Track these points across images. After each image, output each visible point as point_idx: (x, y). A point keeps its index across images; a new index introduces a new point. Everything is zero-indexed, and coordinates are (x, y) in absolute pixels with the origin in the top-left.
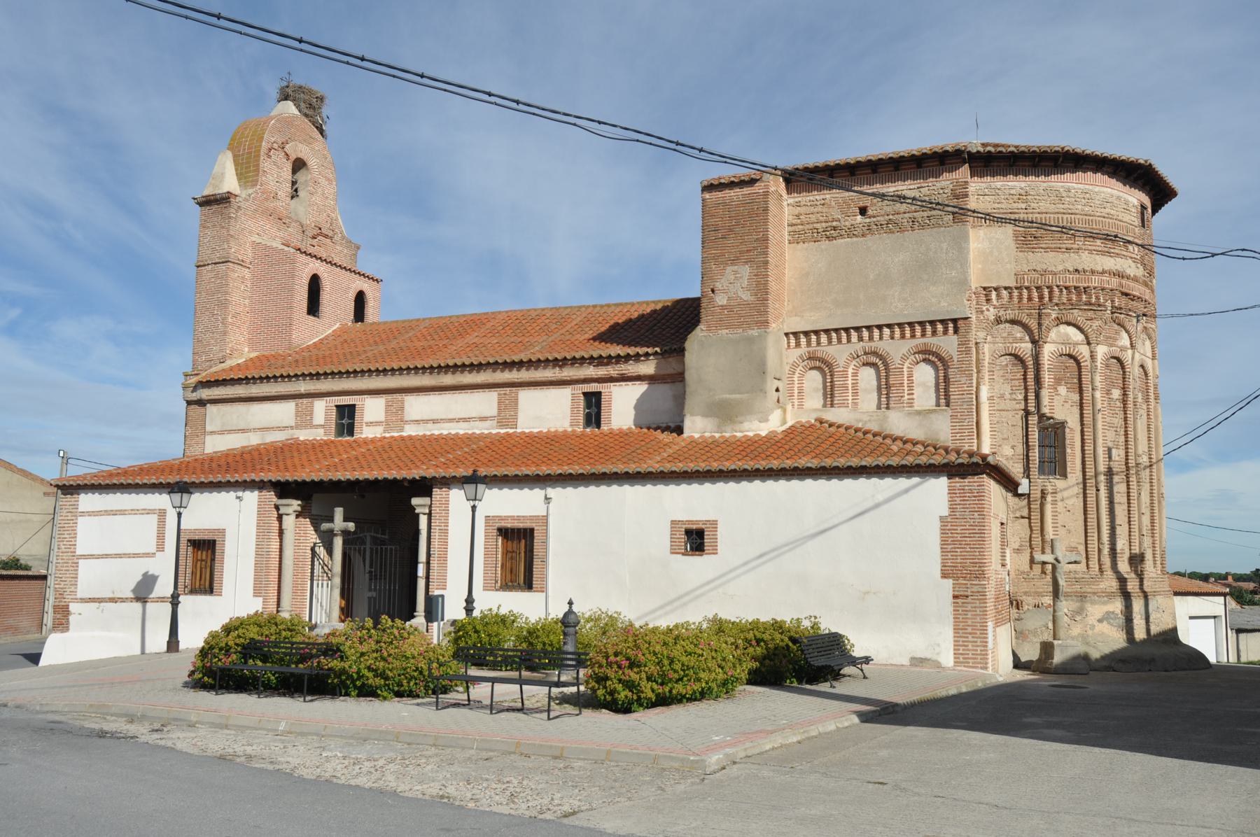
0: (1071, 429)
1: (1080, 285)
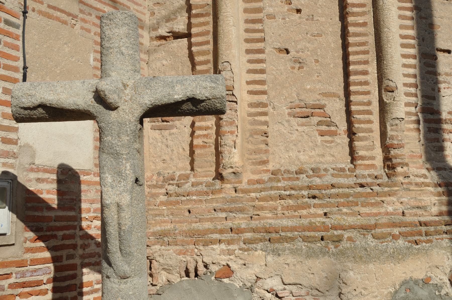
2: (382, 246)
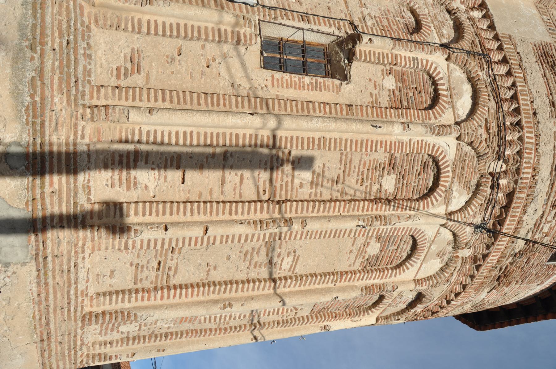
0: (339, 88)
1: (523, 115)
2: (26, 82)
